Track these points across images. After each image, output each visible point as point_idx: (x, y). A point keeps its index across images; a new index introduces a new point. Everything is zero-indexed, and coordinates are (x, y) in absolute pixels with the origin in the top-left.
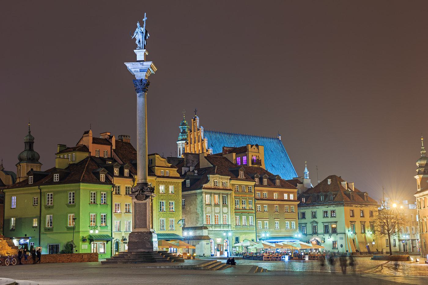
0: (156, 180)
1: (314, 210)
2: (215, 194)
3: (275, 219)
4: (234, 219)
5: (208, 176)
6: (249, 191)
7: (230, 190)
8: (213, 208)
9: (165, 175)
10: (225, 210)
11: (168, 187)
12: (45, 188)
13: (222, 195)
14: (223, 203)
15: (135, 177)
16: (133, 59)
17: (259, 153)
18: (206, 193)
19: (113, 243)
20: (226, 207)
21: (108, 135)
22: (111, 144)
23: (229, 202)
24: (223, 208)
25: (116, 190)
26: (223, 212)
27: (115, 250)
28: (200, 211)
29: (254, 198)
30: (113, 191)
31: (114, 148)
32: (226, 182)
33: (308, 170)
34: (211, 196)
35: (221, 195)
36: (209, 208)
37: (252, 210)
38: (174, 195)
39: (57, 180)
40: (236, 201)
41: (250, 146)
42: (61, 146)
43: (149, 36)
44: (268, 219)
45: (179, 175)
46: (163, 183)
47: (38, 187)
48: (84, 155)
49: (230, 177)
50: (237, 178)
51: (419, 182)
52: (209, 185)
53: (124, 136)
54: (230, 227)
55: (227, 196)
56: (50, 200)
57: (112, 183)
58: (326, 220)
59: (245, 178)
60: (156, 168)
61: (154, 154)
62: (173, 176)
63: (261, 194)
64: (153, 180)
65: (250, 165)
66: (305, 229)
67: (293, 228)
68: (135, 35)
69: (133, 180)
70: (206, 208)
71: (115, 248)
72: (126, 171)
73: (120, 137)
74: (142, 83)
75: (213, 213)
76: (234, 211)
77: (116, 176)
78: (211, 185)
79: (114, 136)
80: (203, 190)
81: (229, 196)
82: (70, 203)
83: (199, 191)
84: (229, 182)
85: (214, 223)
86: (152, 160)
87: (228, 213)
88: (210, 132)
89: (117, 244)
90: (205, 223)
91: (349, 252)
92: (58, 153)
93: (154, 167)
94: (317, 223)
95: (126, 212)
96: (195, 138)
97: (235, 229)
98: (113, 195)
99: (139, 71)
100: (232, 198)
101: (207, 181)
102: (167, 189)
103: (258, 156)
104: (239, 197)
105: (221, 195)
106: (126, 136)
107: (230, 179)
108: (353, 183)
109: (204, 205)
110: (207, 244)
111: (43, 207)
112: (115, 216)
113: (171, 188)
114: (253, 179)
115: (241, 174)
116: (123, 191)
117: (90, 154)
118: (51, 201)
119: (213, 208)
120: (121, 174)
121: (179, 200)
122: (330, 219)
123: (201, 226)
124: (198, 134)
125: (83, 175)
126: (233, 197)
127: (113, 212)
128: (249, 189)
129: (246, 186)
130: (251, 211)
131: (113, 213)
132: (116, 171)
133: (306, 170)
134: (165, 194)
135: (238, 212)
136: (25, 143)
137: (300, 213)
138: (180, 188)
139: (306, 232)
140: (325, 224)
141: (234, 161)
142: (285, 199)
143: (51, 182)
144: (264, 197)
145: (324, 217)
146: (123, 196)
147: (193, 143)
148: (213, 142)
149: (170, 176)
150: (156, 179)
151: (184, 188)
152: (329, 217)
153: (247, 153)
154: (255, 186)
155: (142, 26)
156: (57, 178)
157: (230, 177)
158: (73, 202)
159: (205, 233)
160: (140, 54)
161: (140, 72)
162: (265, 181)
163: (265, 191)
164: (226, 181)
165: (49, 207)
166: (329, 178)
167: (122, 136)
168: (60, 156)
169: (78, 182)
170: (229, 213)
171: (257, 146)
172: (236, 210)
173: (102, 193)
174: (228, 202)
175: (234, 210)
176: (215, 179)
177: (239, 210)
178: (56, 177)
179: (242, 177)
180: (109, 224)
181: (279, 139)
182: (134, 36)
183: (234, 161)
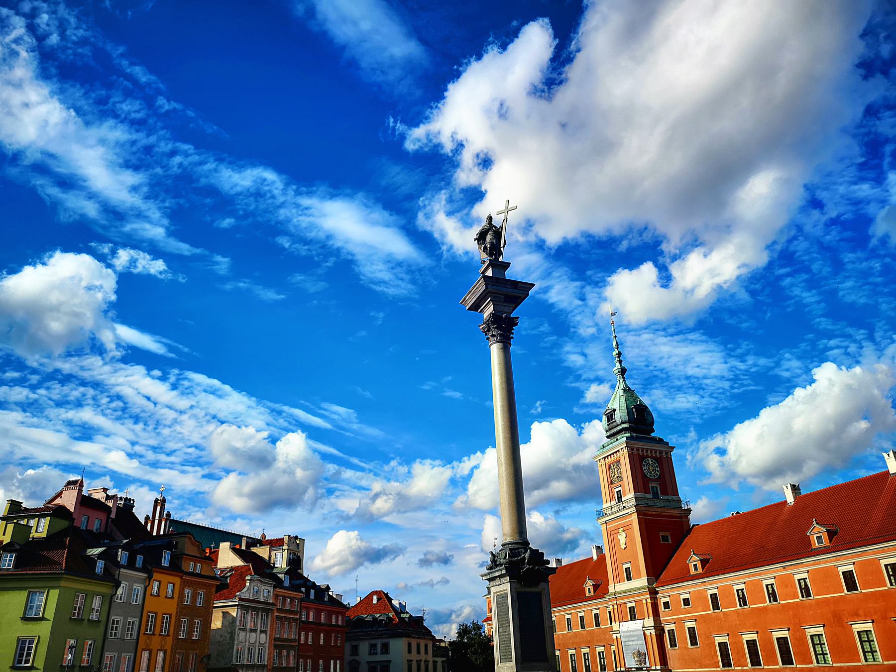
1: (354, 643)
8: (248, 634)
31: (113, 515)
57: (116, 577)
70: (238, 635)
72: (140, 559)
75: (247, 644)
85: (245, 662)
94: (358, 663)
120: (131, 565)
122: (380, 658)
123: (227, 666)
145: (370, 654)
152: (379, 653)
164: (269, 589)
166: (373, 593)
168: (17, 521)
174: (267, 624)
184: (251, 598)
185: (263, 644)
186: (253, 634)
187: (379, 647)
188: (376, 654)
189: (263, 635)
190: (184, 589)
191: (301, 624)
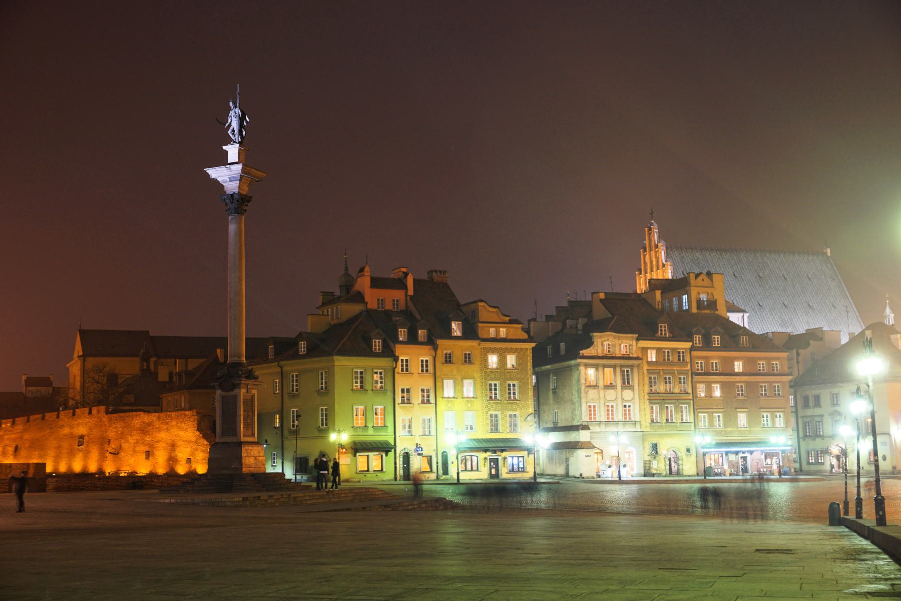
0: (481, 347)
2: (604, 366)
3: (738, 410)
4: (648, 410)
5: (591, 334)
6: (679, 360)
7: (637, 358)
9: (498, 337)
10: (628, 394)
11: (505, 358)
12: (291, 367)
13: (621, 368)
14: (624, 383)
15: (438, 343)
16: (222, 160)
17: (713, 287)
18: (587, 366)
19: (398, 455)
20: (630, 389)
21: (403, 272)
22: (405, 287)
23: (635, 382)
24: (622, 391)
25: (402, 365)
26: (622, 399)
27: (402, 466)
28: (577, 398)
29: (690, 372)
30: (396, 367)
31: (411, 292)
32: (630, 345)
33: (893, 311)
35: (618, 370)
36: (592, 393)
37: (687, 393)
38: (517, 371)
39: (304, 351)
40: (650, 378)
41: (692, 276)
42: (325, 294)
43: (248, 120)
44: (722, 410)
45: (526, 336)
46: (493, 351)
47: (276, 364)
48: (355, 309)
49: (637, 336)
50: (655, 336)
52: (593, 351)
53: (436, 271)
54: (638, 426)
56: (295, 383)
59: (671, 336)
60: (480, 325)
61: (475, 302)
62: (514, 337)
63: (707, 364)
64: (473, 347)
65: (694, 310)
66: (821, 427)
67: (766, 425)
68: (229, 121)
69: (434, 348)
70: (586, 393)
71: (402, 463)
72: (422, 333)
73: (430, 274)
74: (233, 199)
75: (602, 401)
76: (647, 397)
77: (402, 343)
78: (597, 351)
79: (410, 274)
80: (579, 360)
81: (635, 370)
82: (322, 387)
83: (573, 362)
85: (603, 419)
86: (474, 311)
88: (681, 248)
89: (407, 457)
90: (585, 418)
91: (897, 469)
92: (320, 307)
93: (476, 324)
95: (423, 402)
96: (651, 262)
97: (650, 429)
98: (396, 375)
99: (228, 180)
100: (643, 373)
101: (589, 343)
102: (502, 361)
103: (712, 294)
104: (658, 371)
105: (618, 370)
106: (440, 272)
107: (638, 339)
109: (583, 387)
110: (587, 456)
111: (286, 396)
112: (400, 410)
113: (511, 360)
114: (689, 338)
115: (664, 328)
116: (415, 367)
117: (367, 307)
118: (297, 385)
119: (602, 392)
120: (413, 340)
121: (528, 380)
124: (656, 255)
125: (342, 342)
126: (645, 372)
127: (397, 402)
128: (679, 356)
129: (673, 349)
130: (684, 396)
131: (397, 405)
132: (402, 334)
133: (888, 310)
134: (498, 370)
135: (654, 397)
136: (340, 286)
137: (812, 396)
138: (529, 359)
139: (823, 433)
141: (658, 305)
142: (736, 370)
143: (296, 356)
144: (713, 370)
146: (416, 375)
147: (649, 271)
148: (687, 268)
149: (508, 338)
150: (479, 345)
151: (539, 357)
153: (687, 288)
154: (692, 349)
155: (236, 107)
156: (379, 346)
157: (637, 336)
158: (326, 388)
159: (583, 436)
160: (233, 151)
161: (230, 181)
162: (716, 339)
163: (715, 358)
164: (631, 342)
165: (294, 396)
167: (432, 271)
169: (330, 354)
171: (709, 274)
172: (651, 395)
173: (375, 370)
174: (633, 380)
175: (646, 394)
176: (604, 342)
177: (656, 395)
178: (302, 346)
179: (665, 334)
180: (390, 424)
181: (826, 253)
182: (228, 124)
183: (658, 305)
184: (600, 355)
185: (630, 400)
187: (811, 400)
190: (486, 355)
191: (694, 376)
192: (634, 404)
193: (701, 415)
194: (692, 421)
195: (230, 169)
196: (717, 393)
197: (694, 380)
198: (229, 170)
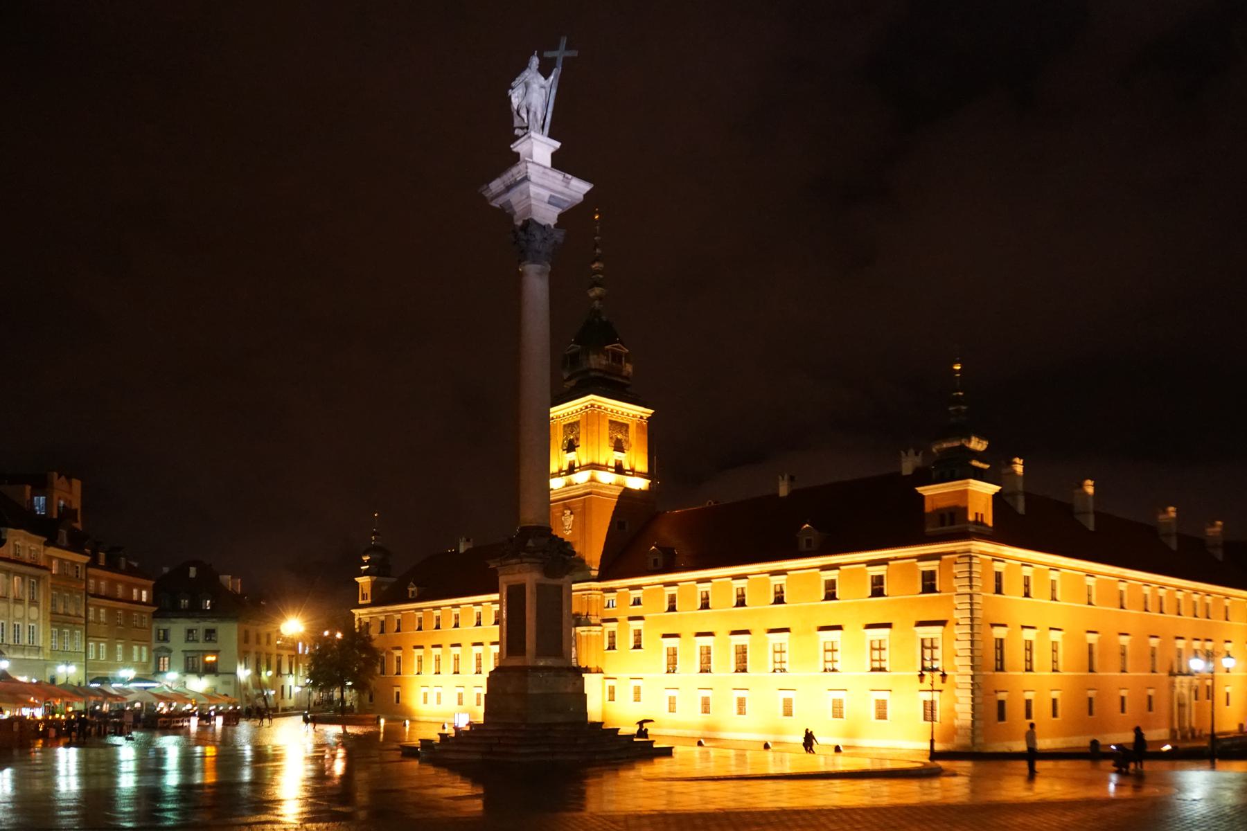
2: (16, 574)
8: (12, 606)
24: (29, 607)
26: (29, 618)
34: (23, 580)
37: (81, 617)
44: (106, 640)
49: (45, 539)
51: (367, 590)
55: (38, 582)
58: (190, 646)
84: (42, 550)
87: (37, 622)
99: (546, 199)
108: (239, 580)
119: (12, 606)
122: (201, 646)
126: (49, 586)
130: (77, 619)
140: (189, 655)
161: (549, 203)
170: (41, 620)
174: (38, 595)
186: (19, 607)
188: (197, 641)
189: (34, 609)
192: (39, 625)
193: (91, 644)
194: (83, 650)
195: (568, 183)
196: (103, 617)
197: (88, 602)
198: (564, 184)
